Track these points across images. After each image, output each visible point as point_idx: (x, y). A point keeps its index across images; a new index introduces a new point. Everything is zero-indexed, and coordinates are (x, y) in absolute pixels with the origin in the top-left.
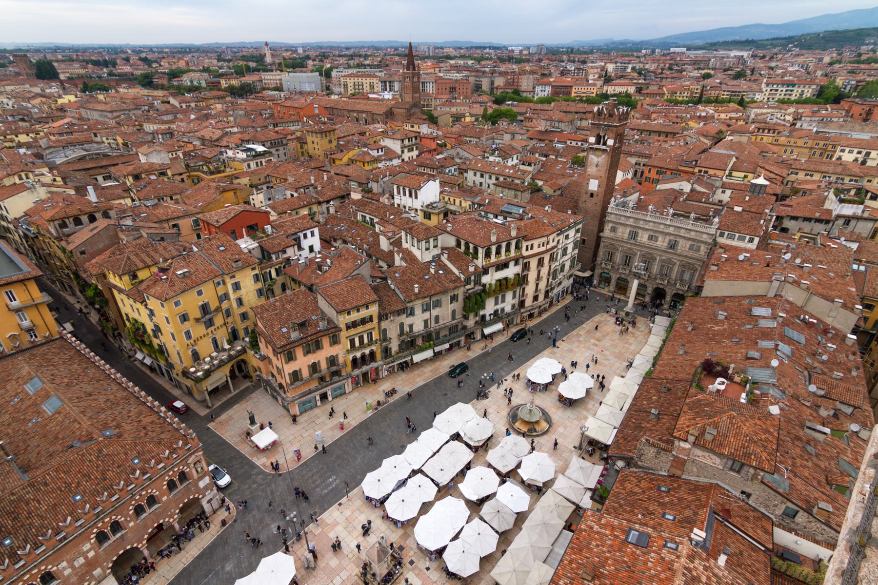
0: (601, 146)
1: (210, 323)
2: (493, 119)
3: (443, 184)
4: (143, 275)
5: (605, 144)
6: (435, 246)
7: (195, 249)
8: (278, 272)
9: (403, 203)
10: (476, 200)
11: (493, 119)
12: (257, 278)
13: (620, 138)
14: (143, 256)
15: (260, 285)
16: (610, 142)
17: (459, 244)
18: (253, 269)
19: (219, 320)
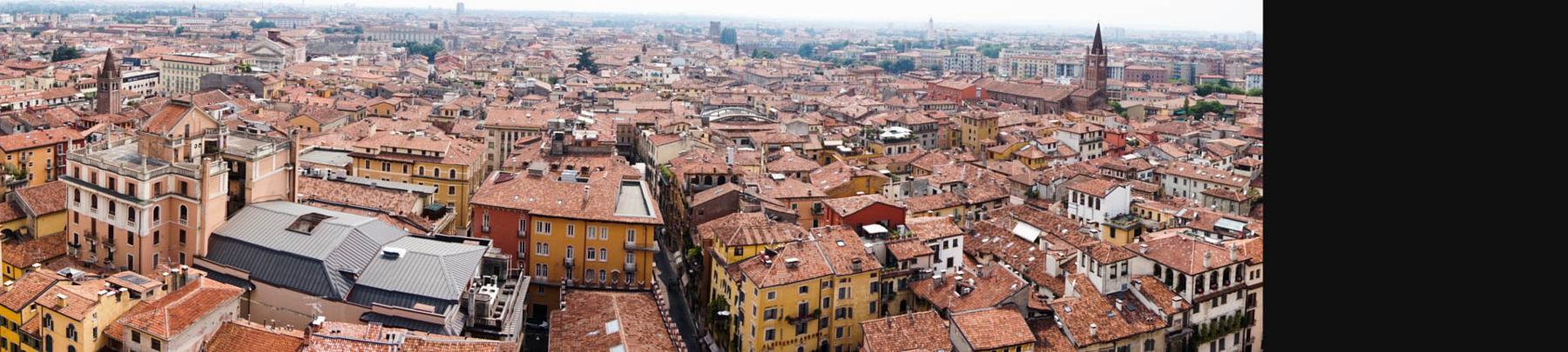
1: (802, 330)
2: (1199, 112)
3: (1135, 191)
4: (748, 252)
6: (1124, 274)
7: (811, 238)
8: (902, 285)
9: (1080, 214)
10: (1181, 213)
11: (1199, 112)
12: (874, 288)
14: (756, 232)
15: (875, 297)
17: (1157, 271)
18: (873, 275)
19: (813, 327)
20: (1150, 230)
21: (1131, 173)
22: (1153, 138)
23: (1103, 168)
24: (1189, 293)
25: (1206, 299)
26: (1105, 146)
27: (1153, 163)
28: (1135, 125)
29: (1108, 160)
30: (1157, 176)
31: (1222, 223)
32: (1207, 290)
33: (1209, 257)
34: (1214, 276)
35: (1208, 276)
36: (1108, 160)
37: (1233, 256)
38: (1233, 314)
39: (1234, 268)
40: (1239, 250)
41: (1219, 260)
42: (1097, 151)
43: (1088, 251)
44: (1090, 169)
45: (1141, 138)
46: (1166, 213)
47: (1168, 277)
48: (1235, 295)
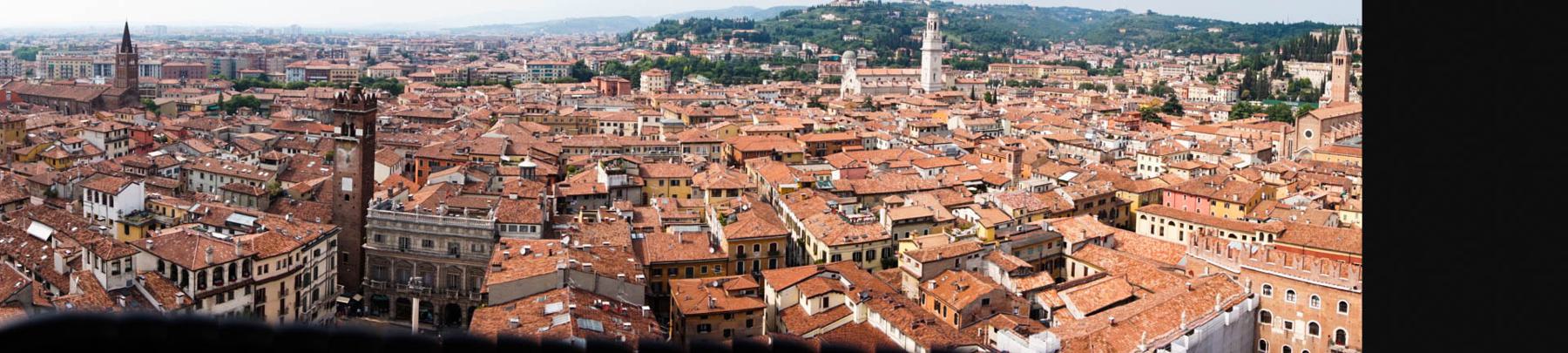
0: (349, 138)
5: (353, 134)
13: (369, 126)
16: (359, 132)
20: (163, 227)
21: (153, 170)
22: (183, 134)
23: (125, 165)
24: (192, 289)
25: (209, 295)
26: (132, 143)
27: (180, 159)
28: (167, 123)
29: (134, 158)
30: (183, 171)
31: (234, 218)
32: (210, 285)
33: (211, 252)
34: (219, 271)
35: (210, 271)
36: (134, 158)
37: (238, 251)
38: (241, 309)
39: (240, 263)
40: (246, 245)
41: (223, 255)
42: (124, 149)
43: (92, 248)
44: (113, 167)
45: (169, 134)
46: (182, 208)
47: (173, 274)
48: (242, 290)
